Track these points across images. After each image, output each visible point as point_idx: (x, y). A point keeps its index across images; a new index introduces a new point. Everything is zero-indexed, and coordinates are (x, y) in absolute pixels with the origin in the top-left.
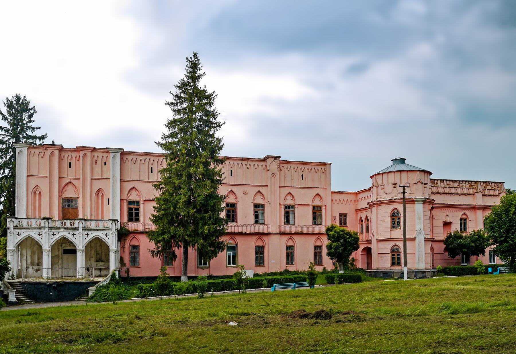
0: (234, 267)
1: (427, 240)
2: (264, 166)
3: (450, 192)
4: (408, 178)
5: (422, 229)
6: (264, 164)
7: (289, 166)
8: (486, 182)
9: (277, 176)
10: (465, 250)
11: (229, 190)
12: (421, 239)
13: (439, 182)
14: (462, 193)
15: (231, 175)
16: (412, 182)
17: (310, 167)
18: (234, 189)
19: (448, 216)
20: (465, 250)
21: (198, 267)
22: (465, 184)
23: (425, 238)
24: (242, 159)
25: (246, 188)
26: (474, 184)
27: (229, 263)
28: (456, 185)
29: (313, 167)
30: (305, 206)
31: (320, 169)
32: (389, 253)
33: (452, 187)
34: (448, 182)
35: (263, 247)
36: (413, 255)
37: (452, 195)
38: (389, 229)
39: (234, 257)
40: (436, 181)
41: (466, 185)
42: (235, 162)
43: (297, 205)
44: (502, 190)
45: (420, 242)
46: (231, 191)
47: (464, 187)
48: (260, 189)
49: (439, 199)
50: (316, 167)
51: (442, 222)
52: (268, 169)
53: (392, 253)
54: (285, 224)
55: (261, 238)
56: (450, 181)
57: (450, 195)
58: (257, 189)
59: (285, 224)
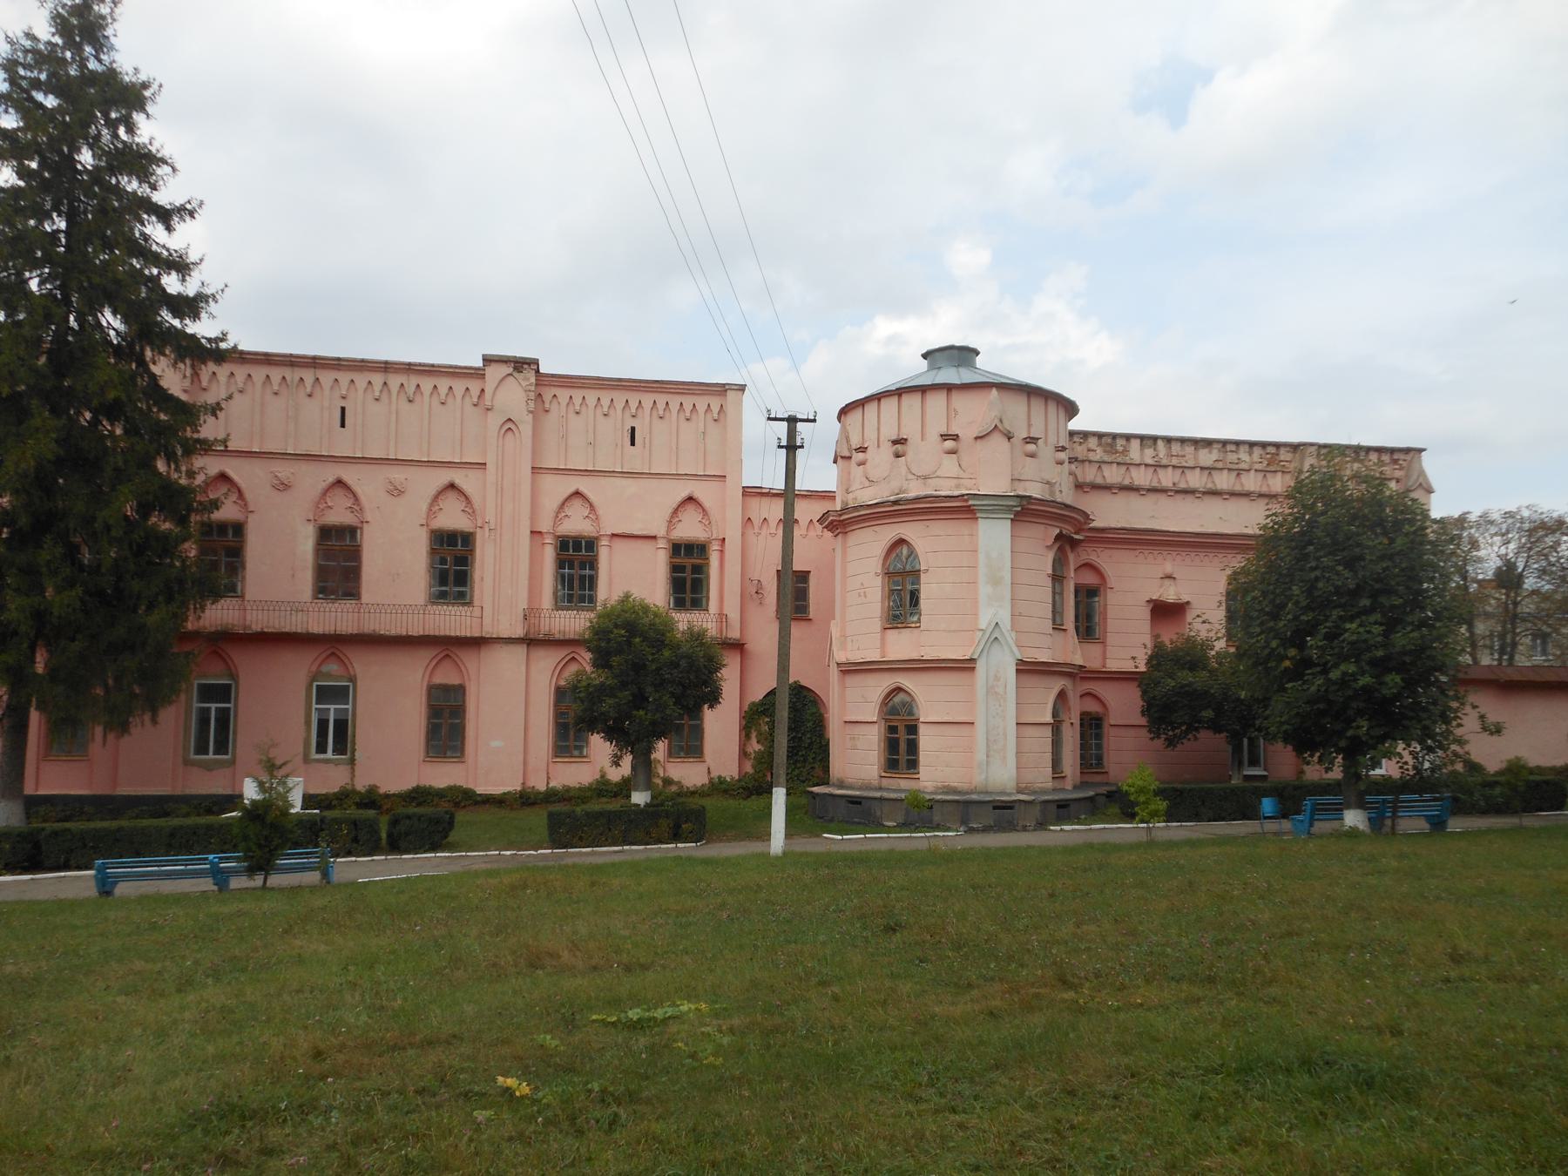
0: (336, 763)
1: (1026, 669)
2: (475, 392)
3: (1183, 485)
4: (950, 414)
5: (1006, 623)
6: (475, 387)
7: (578, 395)
9: (526, 429)
10: (1208, 714)
11: (331, 479)
12: (1000, 666)
13: (1135, 444)
14: (1238, 488)
15: (343, 425)
16: (967, 434)
17: (661, 400)
18: (349, 474)
19: (1169, 577)
20: (1208, 714)
21: (187, 763)
22: (1251, 454)
23: (1021, 662)
24: (386, 367)
25: (398, 475)
26: (1289, 456)
27: (321, 748)
28: (1207, 457)
29: (675, 401)
30: (640, 543)
31: (701, 408)
32: (875, 719)
33: (1191, 464)
34: (1176, 448)
35: (460, 690)
36: (965, 730)
37: (1190, 498)
38: (877, 625)
39: (342, 727)
42: (357, 377)
43: (608, 538)
44: (1415, 477)
45: (997, 678)
46: (339, 483)
47: (1243, 466)
48: (458, 477)
49: (1108, 513)
50: (688, 402)
52: (488, 403)
53: (886, 720)
54: (557, 607)
55: (338, 653)
56: (1183, 441)
57: (1183, 496)
58: (445, 477)
59: (557, 607)
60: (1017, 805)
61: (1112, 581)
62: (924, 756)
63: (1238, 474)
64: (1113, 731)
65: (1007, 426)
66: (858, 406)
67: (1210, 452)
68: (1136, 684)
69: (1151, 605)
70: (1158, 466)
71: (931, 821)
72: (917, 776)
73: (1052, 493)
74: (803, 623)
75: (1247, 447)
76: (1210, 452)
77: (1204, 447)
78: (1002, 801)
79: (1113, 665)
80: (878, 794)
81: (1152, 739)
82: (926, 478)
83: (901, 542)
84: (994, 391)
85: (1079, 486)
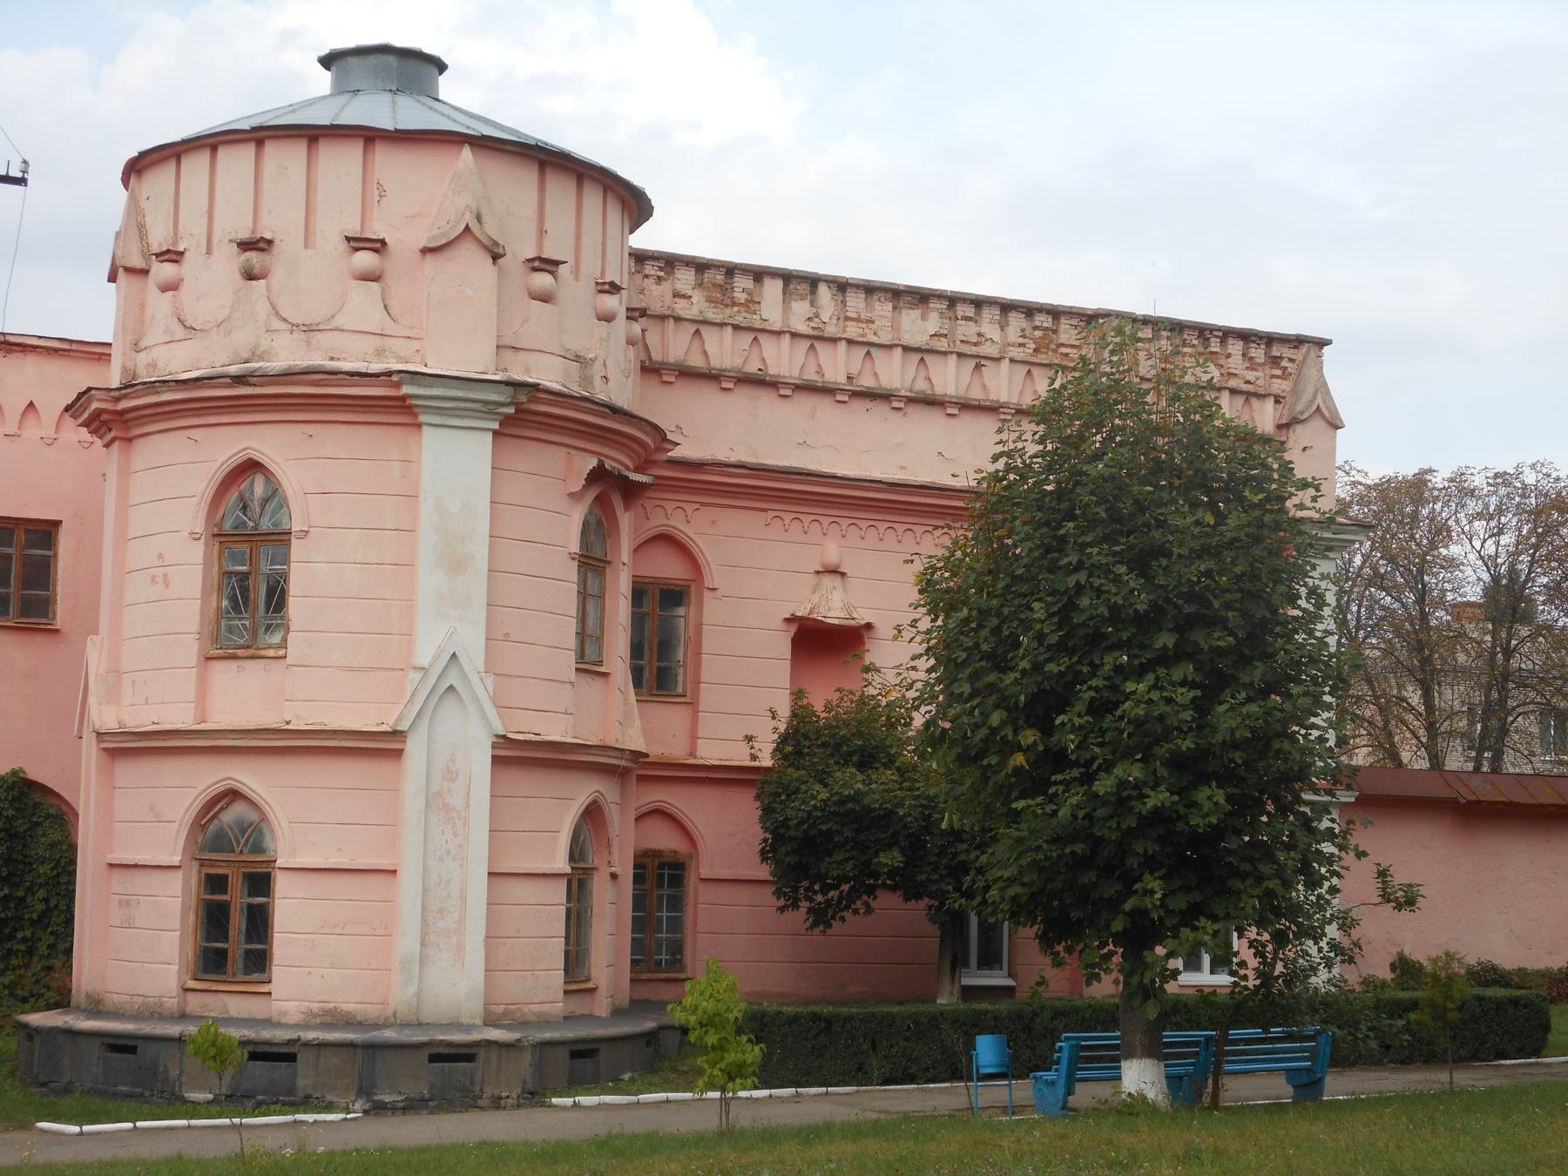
3: (867, 382)
4: (370, 193)
8: (1177, 327)
10: (891, 858)
13: (773, 288)
14: (976, 394)
16: (405, 238)
19: (834, 571)
20: (891, 858)
23: (503, 741)
28: (918, 327)
32: (176, 860)
33: (885, 338)
34: (856, 302)
36: (375, 885)
37: (881, 409)
38: (189, 649)
40: (742, 283)
41: (1013, 334)
44: (1307, 396)
45: (450, 775)
47: (987, 350)
51: (778, 624)
53: (203, 863)
56: (870, 289)
57: (868, 404)
60: (482, 1055)
61: (715, 575)
62: (283, 945)
63: (978, 367)
64: (706, 894)
65: (492, 229)
66: (165, 159)
67: (924, 317)
68: (753, 792)
69: (794, 629)
70: (817, 338)
71: (291, 1090)
72: (264, 989)
73: (586, 381)
74: (39, 638)
75: (996, 311)
76: (924, 317)
77: (912, 306)
78: (450, 1044)
79: (712, 753)
80: (174, 1030)
81: (782, 909)
82: (310, 329)
83: (251, 467)
84: (466, 153)
85: (651, 369)
